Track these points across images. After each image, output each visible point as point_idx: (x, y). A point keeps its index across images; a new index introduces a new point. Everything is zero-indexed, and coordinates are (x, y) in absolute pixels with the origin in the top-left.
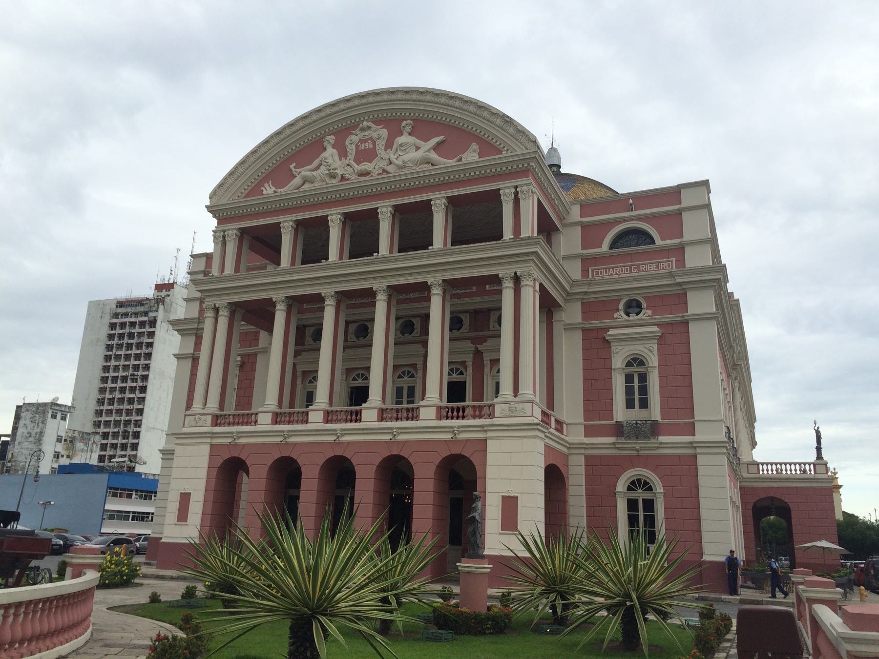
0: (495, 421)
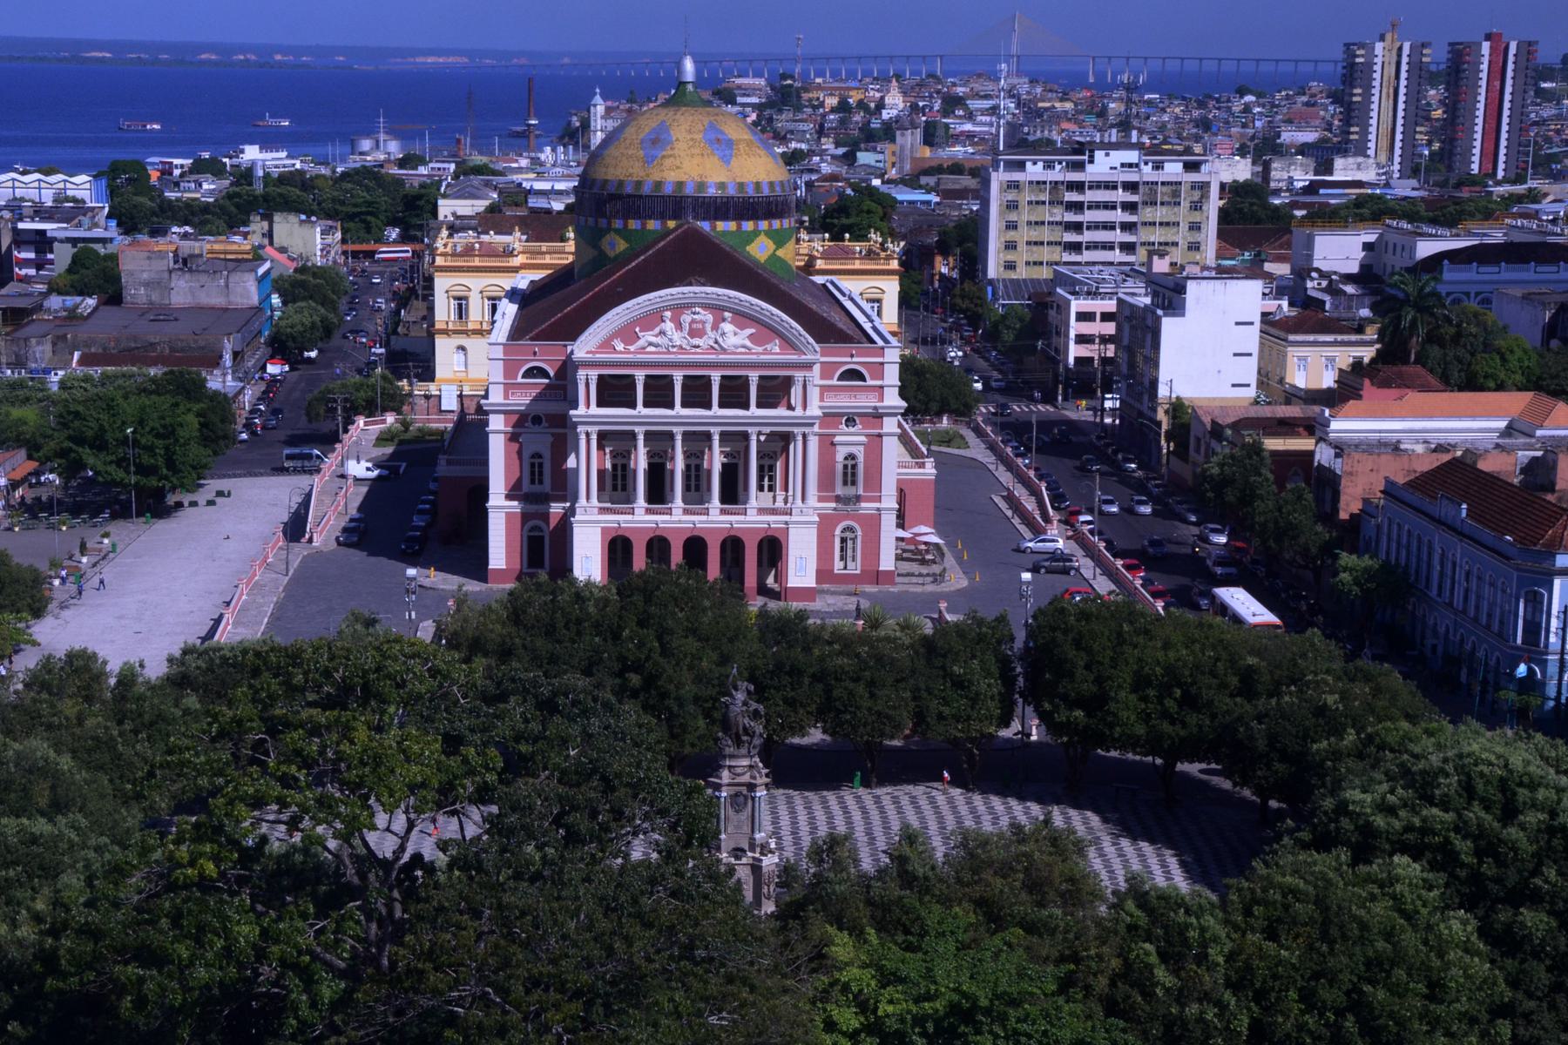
0: (794, 518)
